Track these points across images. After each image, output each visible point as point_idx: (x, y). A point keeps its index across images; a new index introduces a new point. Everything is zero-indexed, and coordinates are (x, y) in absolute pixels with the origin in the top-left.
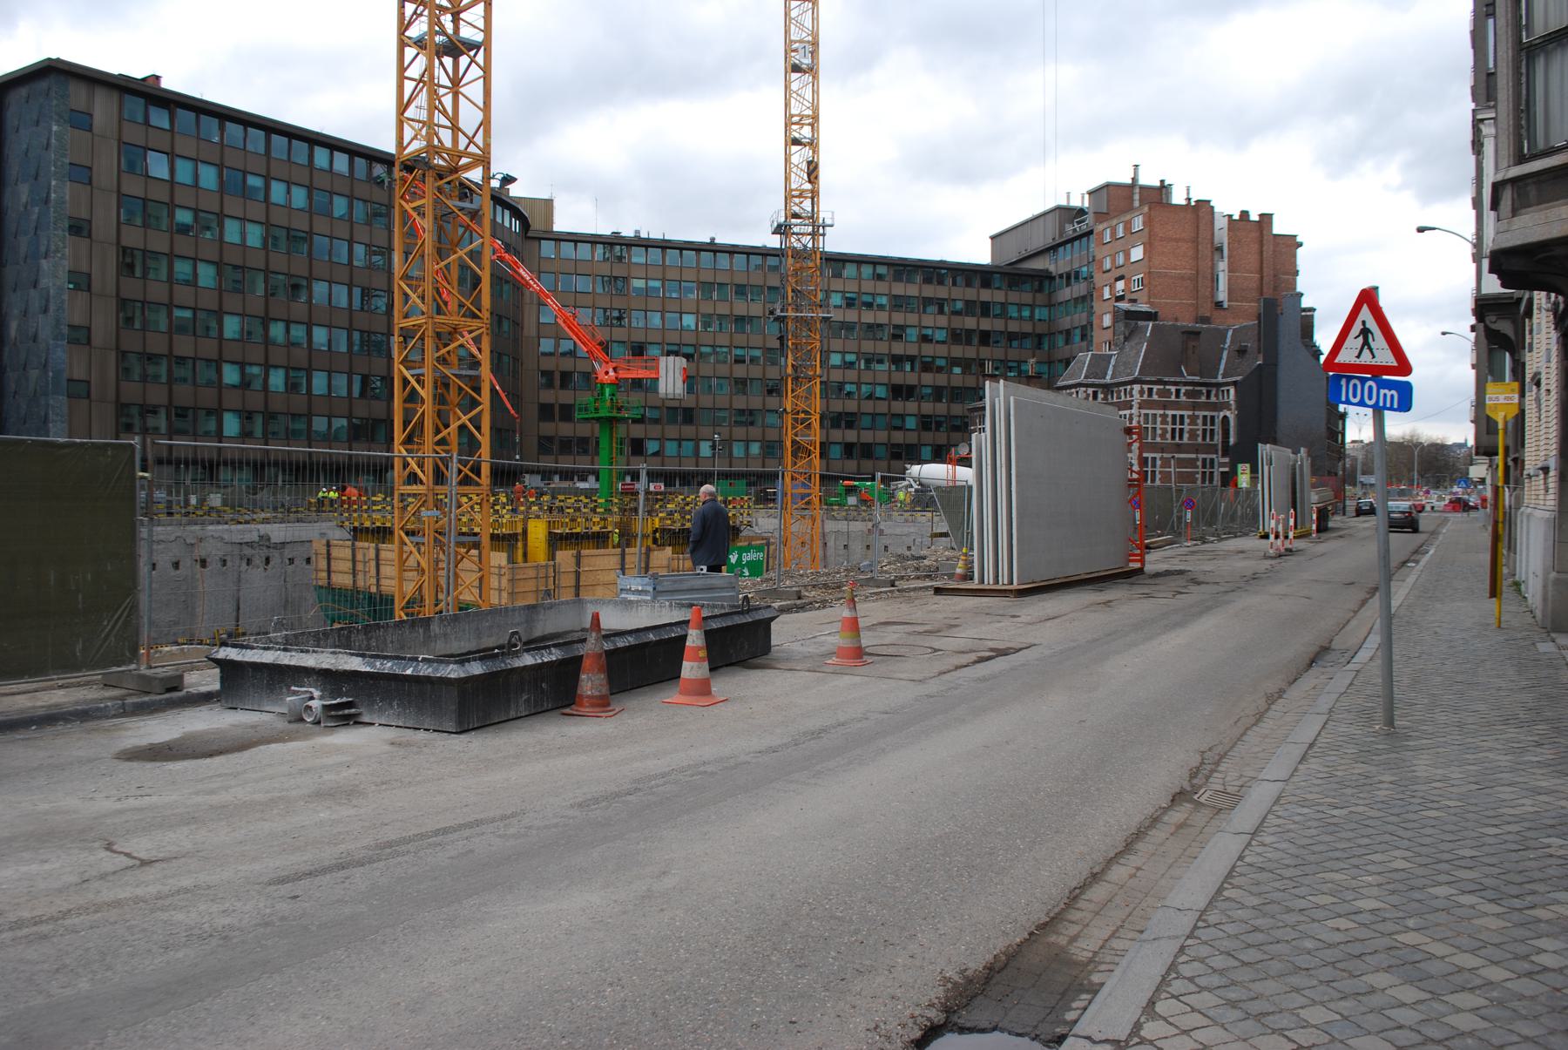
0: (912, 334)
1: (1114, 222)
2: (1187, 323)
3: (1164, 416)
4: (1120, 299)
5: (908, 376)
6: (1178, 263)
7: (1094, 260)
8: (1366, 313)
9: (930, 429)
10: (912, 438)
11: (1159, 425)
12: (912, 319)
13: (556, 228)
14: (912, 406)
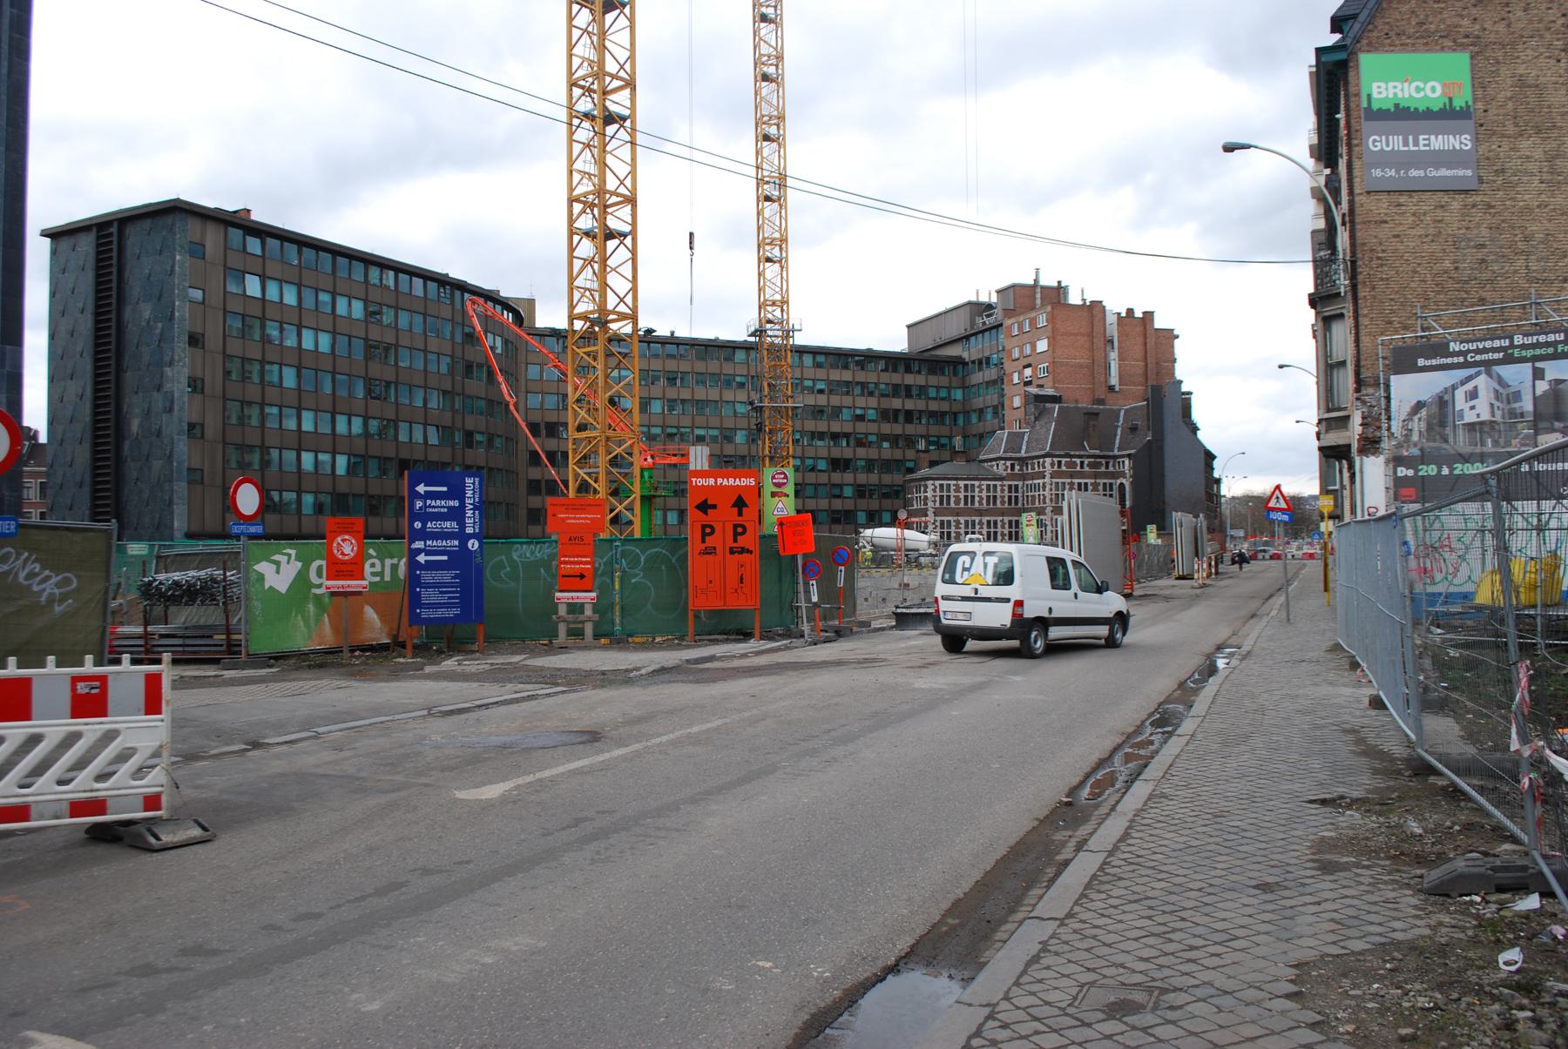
0: (846, 415)
1: (1021, 318)
2: (1085, 404)
4: (1028, 383)
5: (844, 450)
7: (1003, 350)
8: (1277, 492)
9: (865, 497)
10: (849, 505)
12: (848, 401)
13: (538, 325)
14: (848, 477)
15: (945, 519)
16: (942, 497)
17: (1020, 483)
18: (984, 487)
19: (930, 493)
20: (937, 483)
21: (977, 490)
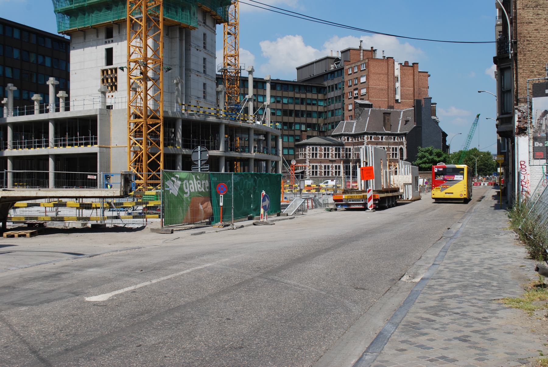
2: (384, 109)
6: (380, 84)
15: (315, 164)
16: (313, 154)
17: (352, 147)
19: (307, 152)
20: (311, 147)
21: (330, 150)
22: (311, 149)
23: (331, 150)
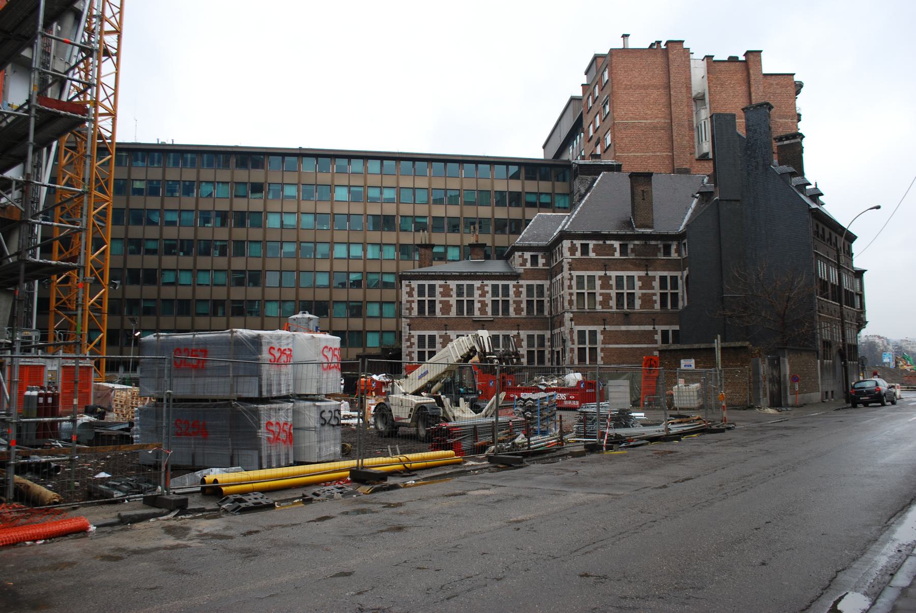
3: (605, 279)
6: (649, 112)
11: (598, 290)
15: (427, 333)
18: (489, 289)
20: (415, 284)
21: (477, 293)
22: (416, 289)
23: (480, 292)
